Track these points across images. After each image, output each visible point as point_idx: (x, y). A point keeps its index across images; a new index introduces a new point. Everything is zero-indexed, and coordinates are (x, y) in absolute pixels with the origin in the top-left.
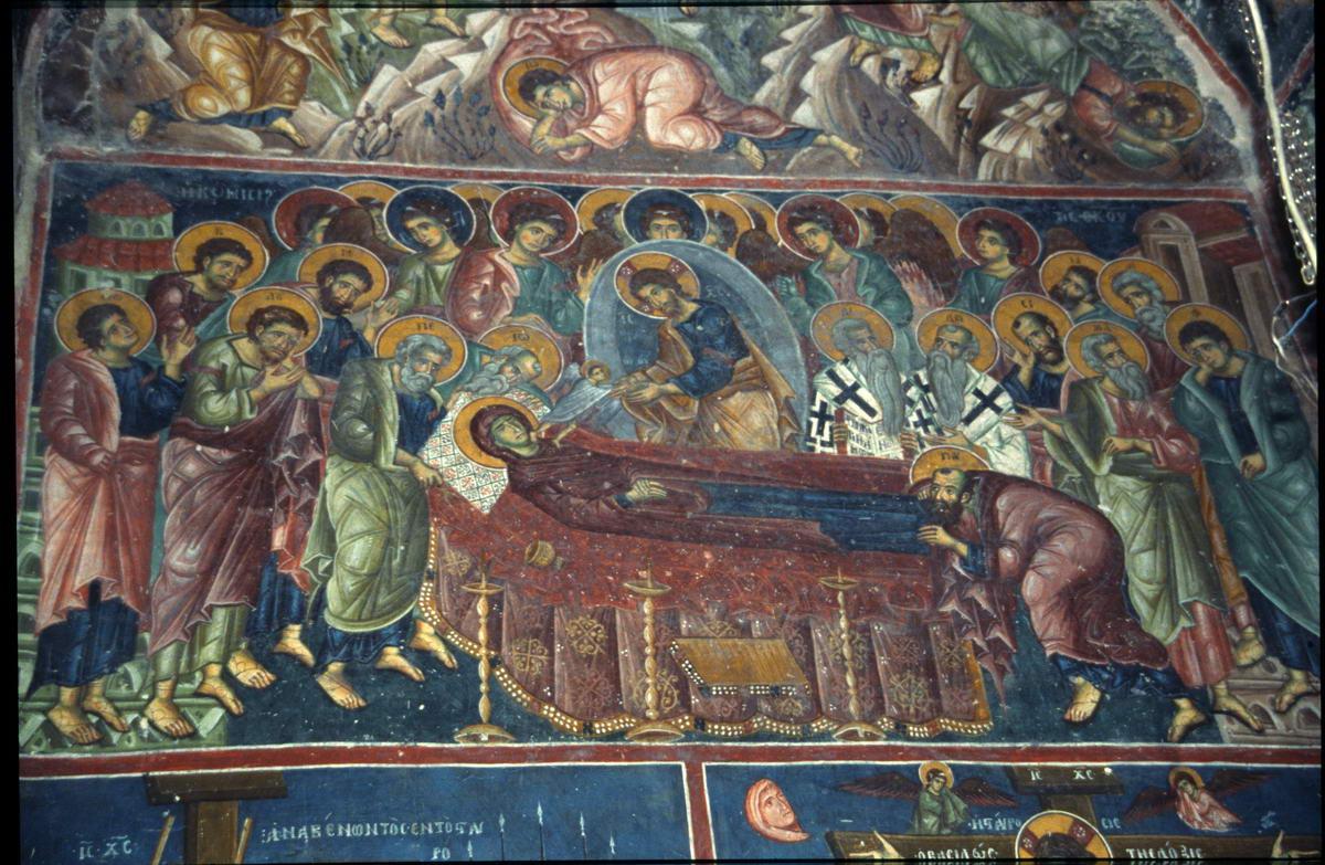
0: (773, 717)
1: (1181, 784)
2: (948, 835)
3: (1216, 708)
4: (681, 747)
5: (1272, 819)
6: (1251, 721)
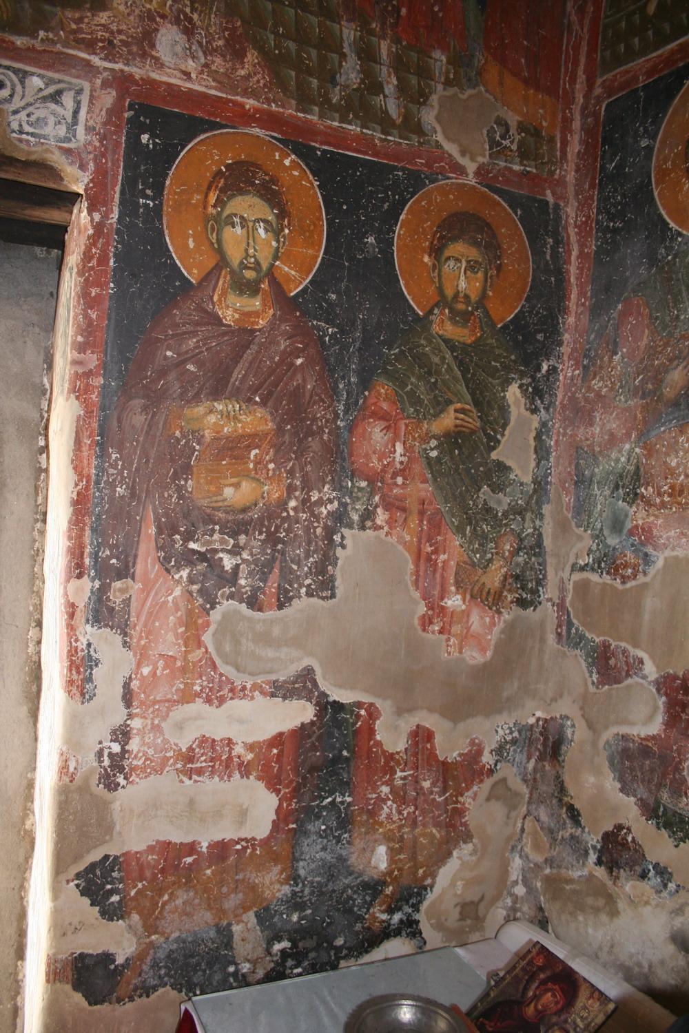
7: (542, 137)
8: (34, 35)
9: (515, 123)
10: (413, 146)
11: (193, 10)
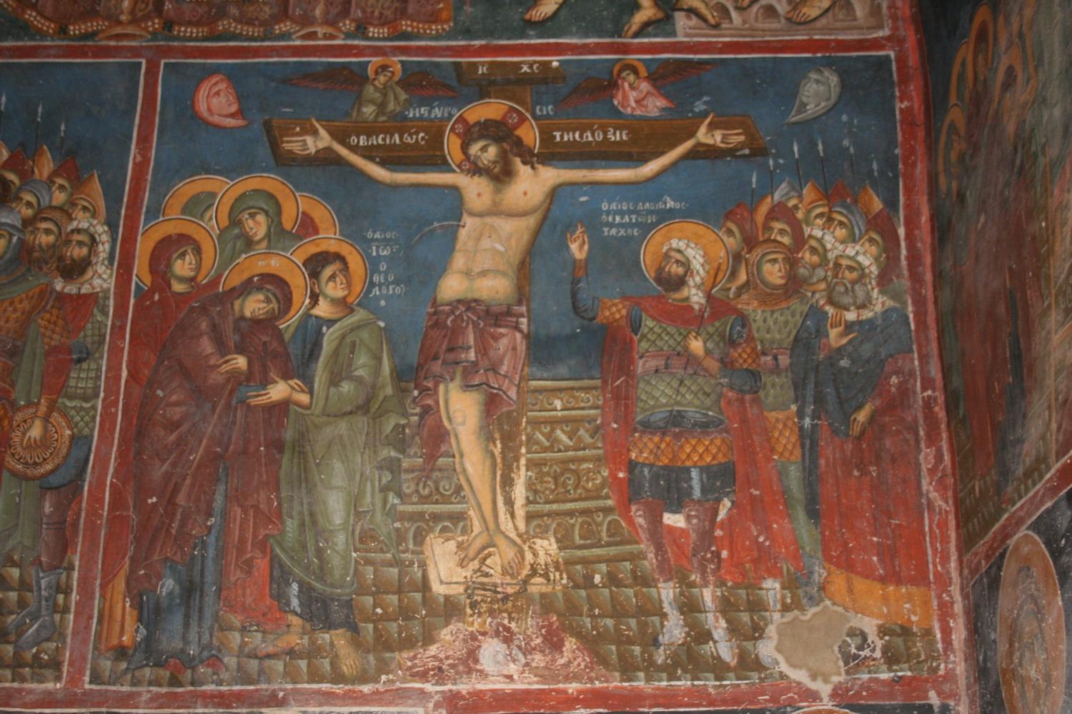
0: (238, 21)
1: (624, 74)
2: (383, 122)
3: (678, 6)
4: (146, 47)
5: (705, 103)
6: (709, 17)
7: (914, 634)
8: (377, 681)
9: (875, 628)
10: (753, 684)
11: (511, 619)
